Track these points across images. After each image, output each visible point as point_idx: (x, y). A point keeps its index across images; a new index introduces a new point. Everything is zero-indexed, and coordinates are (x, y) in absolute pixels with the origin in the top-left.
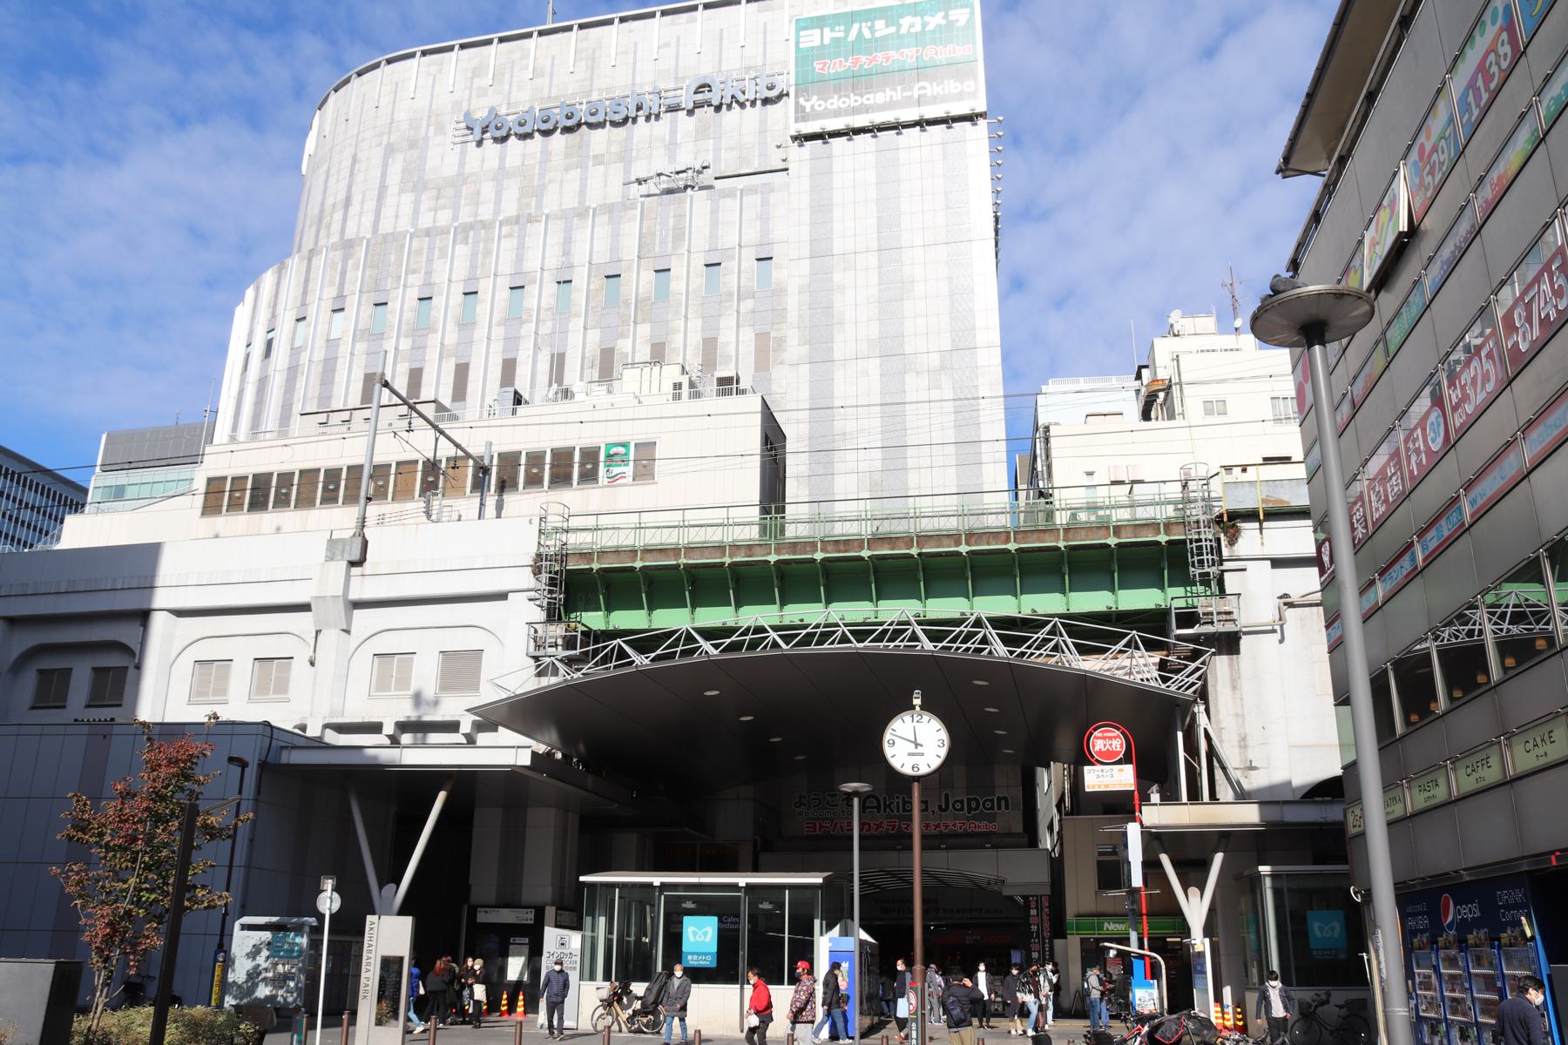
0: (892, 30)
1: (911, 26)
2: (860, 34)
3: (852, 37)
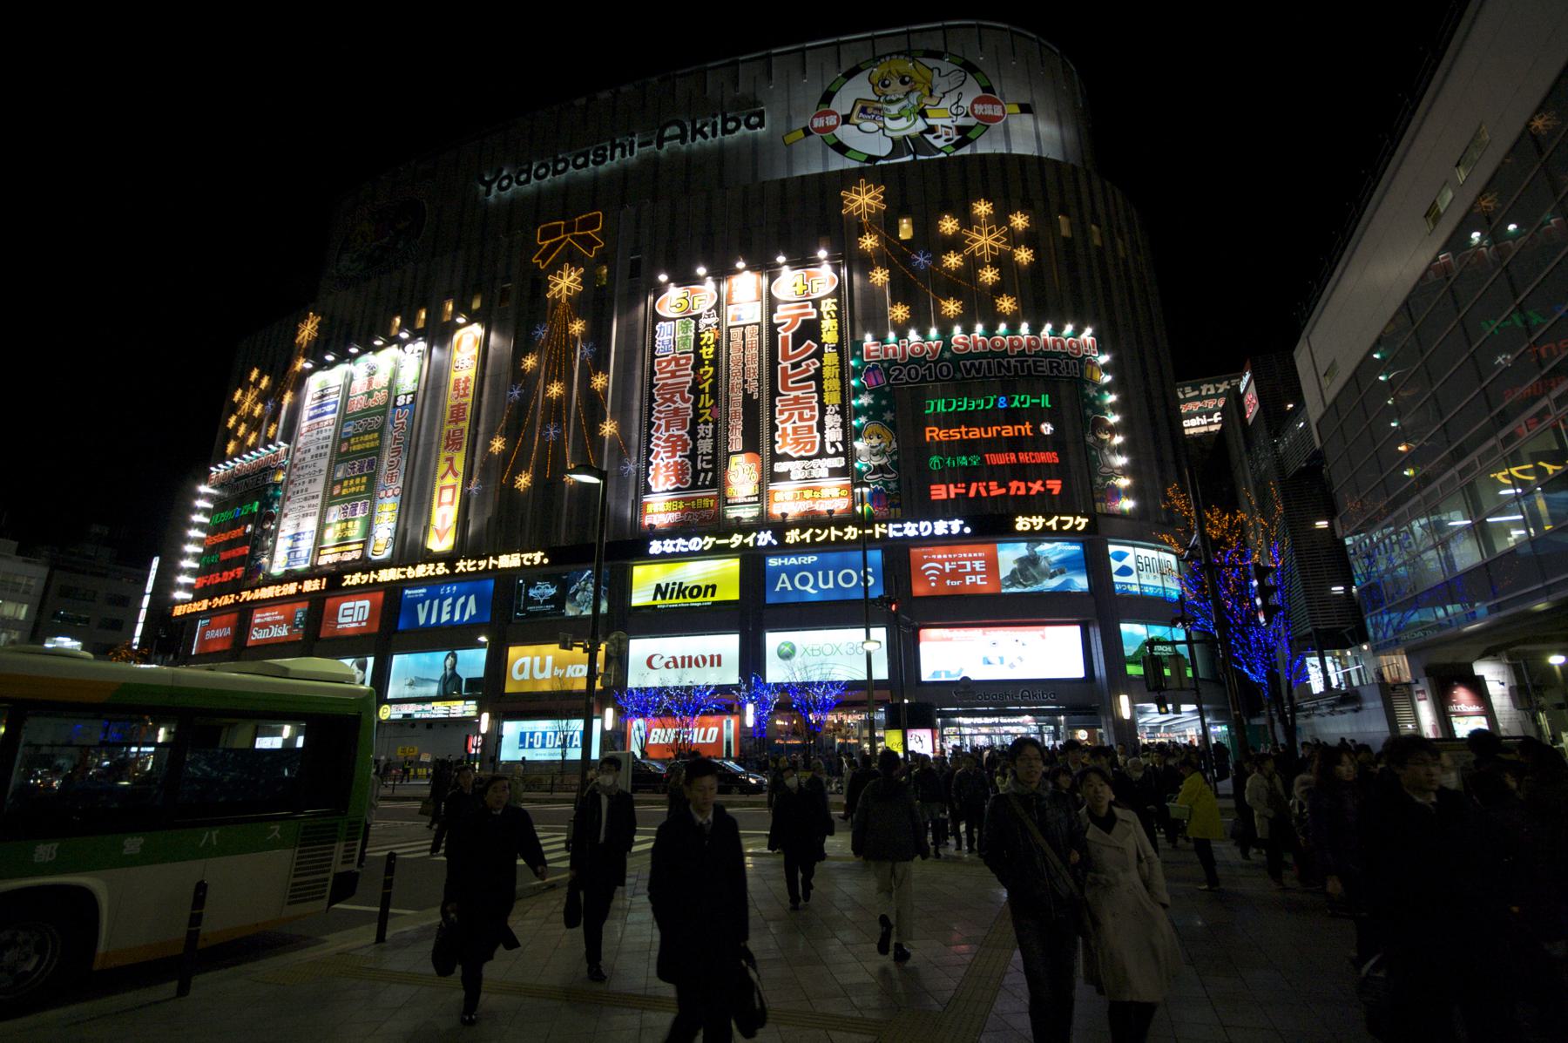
0: (1197, 393)
1: (1208, 390)
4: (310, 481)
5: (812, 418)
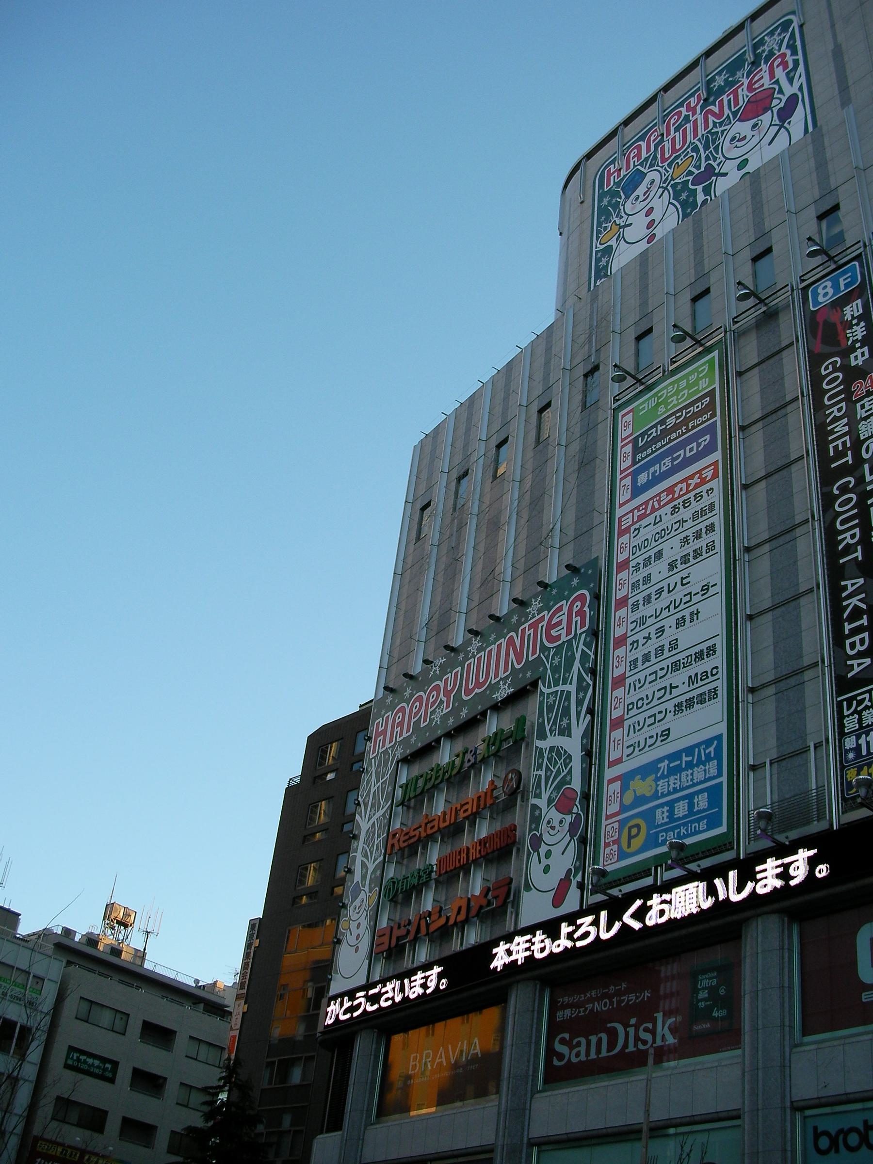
4: (681, 622)
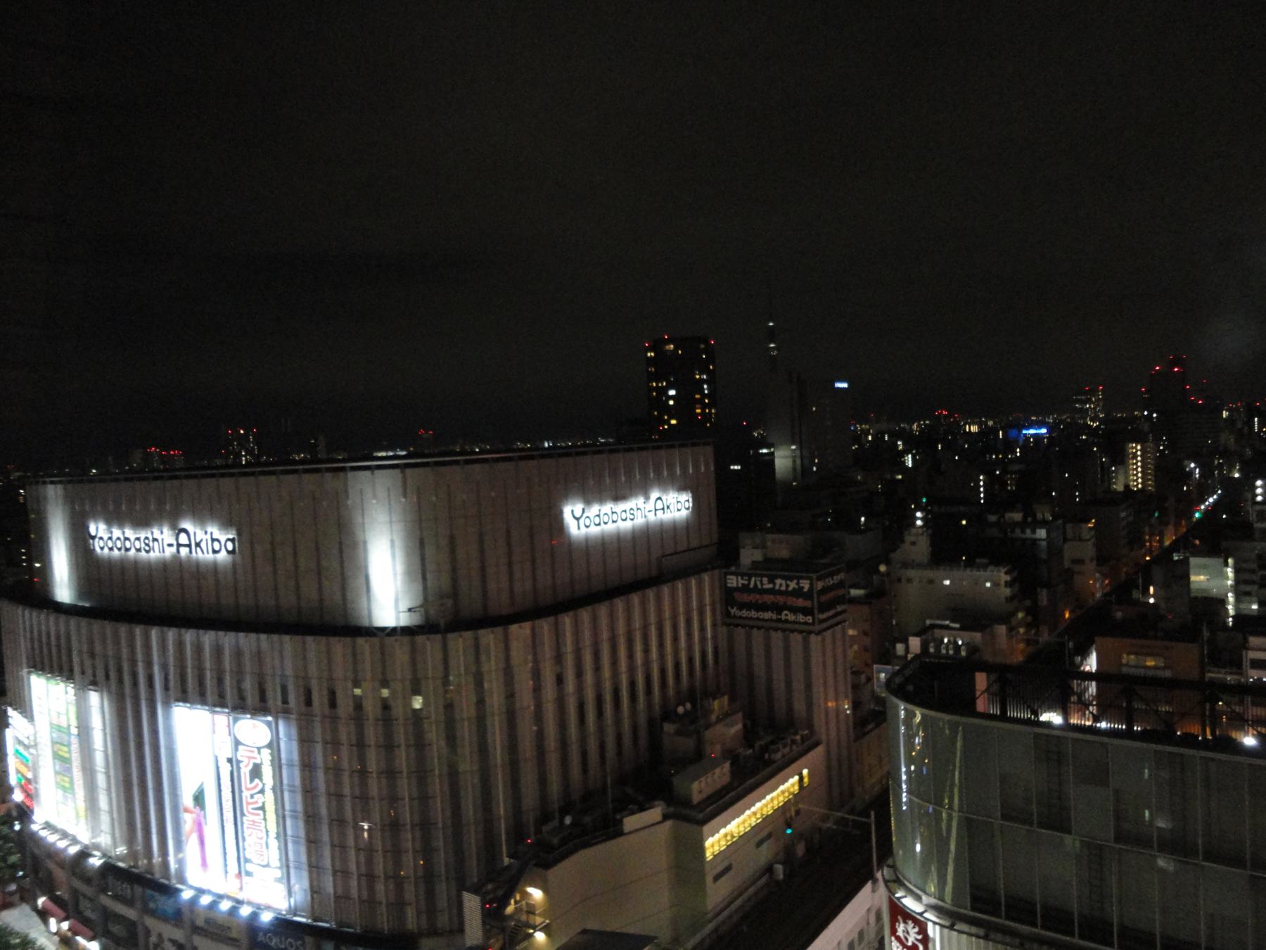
0: (771, 586)
1: (781, 585)
2: (756, 585)
3: (752, 585)
5: (261, 838)
